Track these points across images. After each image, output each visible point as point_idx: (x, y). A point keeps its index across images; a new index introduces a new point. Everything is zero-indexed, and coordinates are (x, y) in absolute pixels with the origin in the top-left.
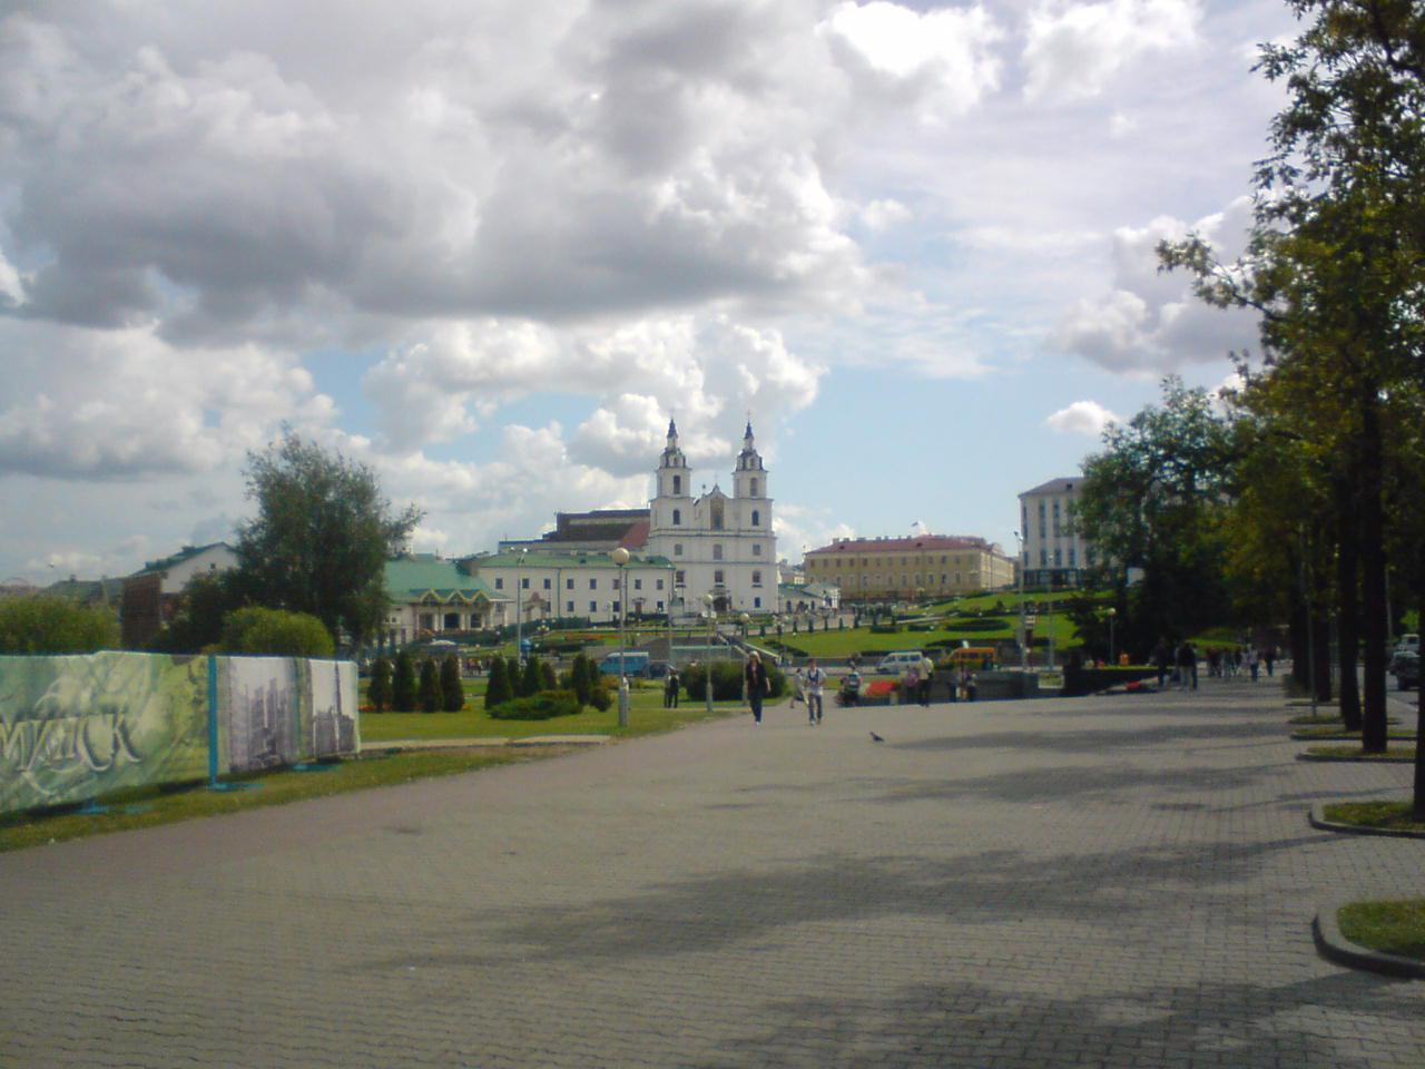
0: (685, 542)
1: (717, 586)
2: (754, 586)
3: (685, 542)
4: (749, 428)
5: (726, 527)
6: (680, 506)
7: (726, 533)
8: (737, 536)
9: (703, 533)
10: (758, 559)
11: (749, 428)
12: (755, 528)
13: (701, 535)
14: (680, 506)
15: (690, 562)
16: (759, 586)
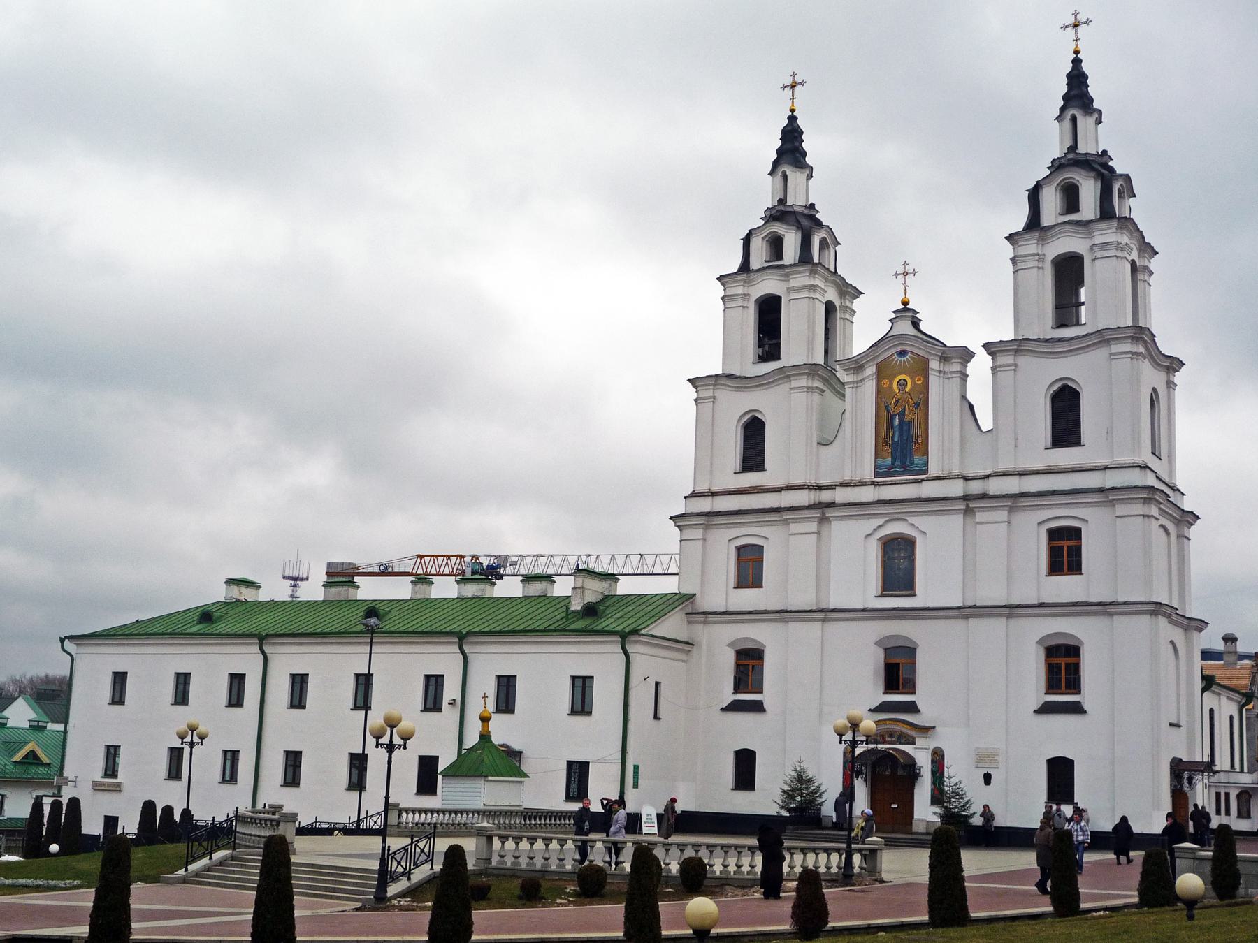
0: (772, 539)
1: (883, 708)
2: (1046, 709)
3: (772, 539)
4: (1077, 79)
5: (933, 469)
6: (764, 402)
7: (929, 489)
8: (966, 498)
9: (840, 495)
10: (1066, 587)
11: (1077, 79)
12: (1066, 456)
13: (832, 505)
14: (764, 402)
15: (780, 615)
16: (1076, 709)
